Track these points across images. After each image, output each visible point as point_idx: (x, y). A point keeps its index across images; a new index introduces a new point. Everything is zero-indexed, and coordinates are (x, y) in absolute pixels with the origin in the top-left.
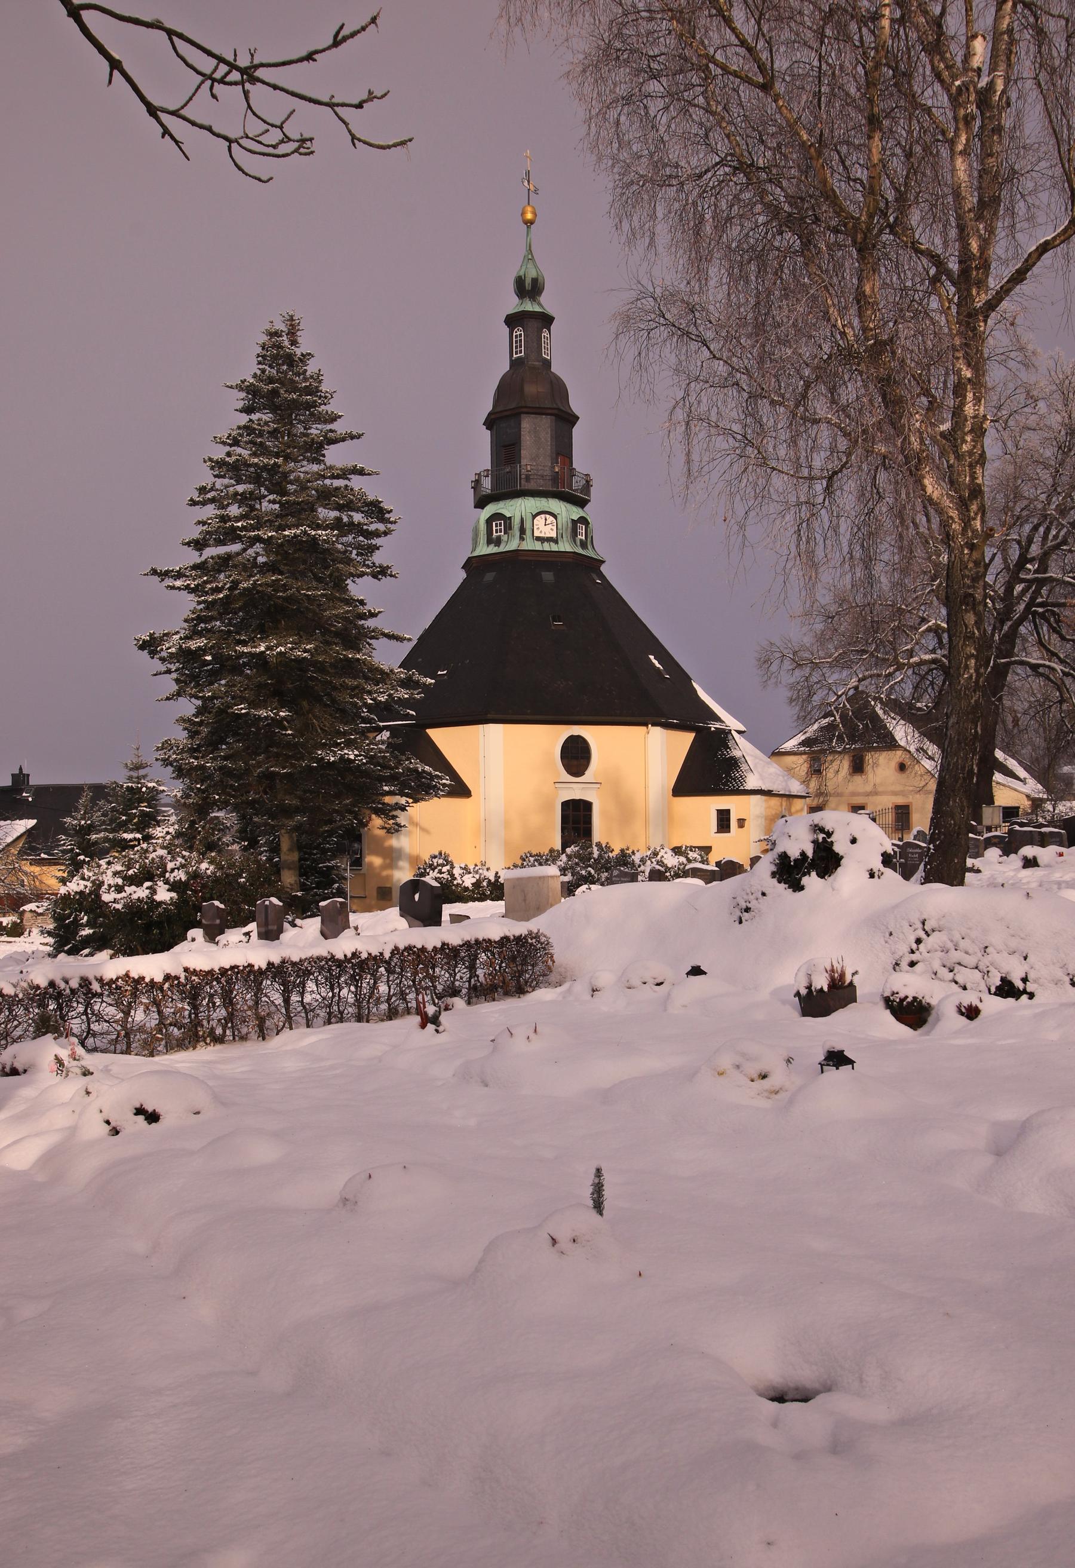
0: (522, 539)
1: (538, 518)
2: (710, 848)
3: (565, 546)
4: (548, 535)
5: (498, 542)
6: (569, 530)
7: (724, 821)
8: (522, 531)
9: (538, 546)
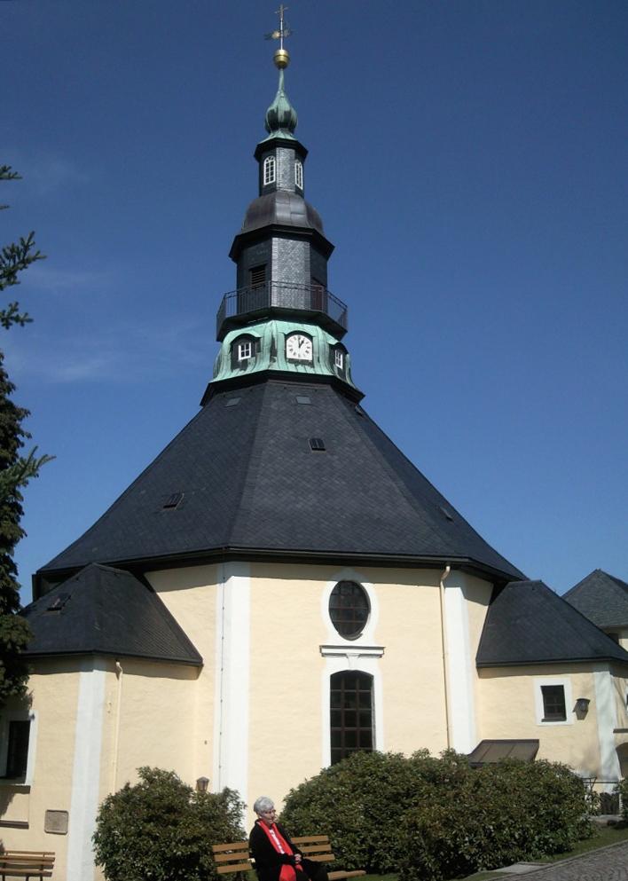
0: (272, 360)
1: (291, 338)
2: (537, 741)
3: (322, 370)
4: (303, 358)
5: (245, 364)
6: (327, 355)
7: (554, 702)
8: (273, 352)
9: (291, 368)
